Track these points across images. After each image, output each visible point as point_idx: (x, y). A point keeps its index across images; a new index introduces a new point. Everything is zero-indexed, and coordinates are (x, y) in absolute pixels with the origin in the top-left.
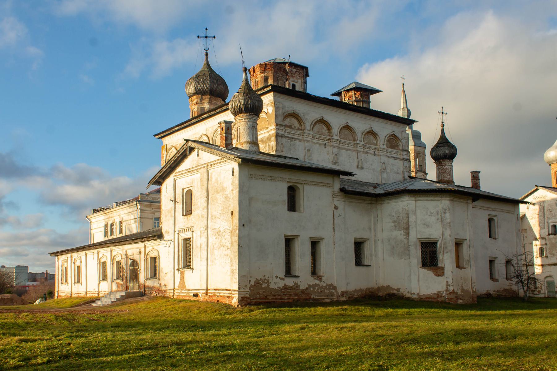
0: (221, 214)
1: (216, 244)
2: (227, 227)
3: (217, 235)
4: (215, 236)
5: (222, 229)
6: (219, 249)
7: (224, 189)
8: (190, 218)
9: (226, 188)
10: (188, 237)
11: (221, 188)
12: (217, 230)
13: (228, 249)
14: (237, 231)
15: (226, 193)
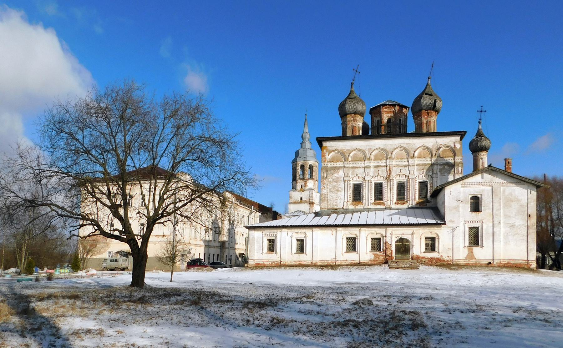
0: (516, 215)
1: (510, 232)
2: (523, 223)
3: (512, 228)
4: (509, 228)
5: (517, 224)
6: (514, 236)
7: (518, 200)
8: (479, 214)
9: (522, 200)
10: (477, 226)
11: (516, 199)
12: (511, 224)
13: (523, 236)
14: (535, 227)
15: (521, 203)
